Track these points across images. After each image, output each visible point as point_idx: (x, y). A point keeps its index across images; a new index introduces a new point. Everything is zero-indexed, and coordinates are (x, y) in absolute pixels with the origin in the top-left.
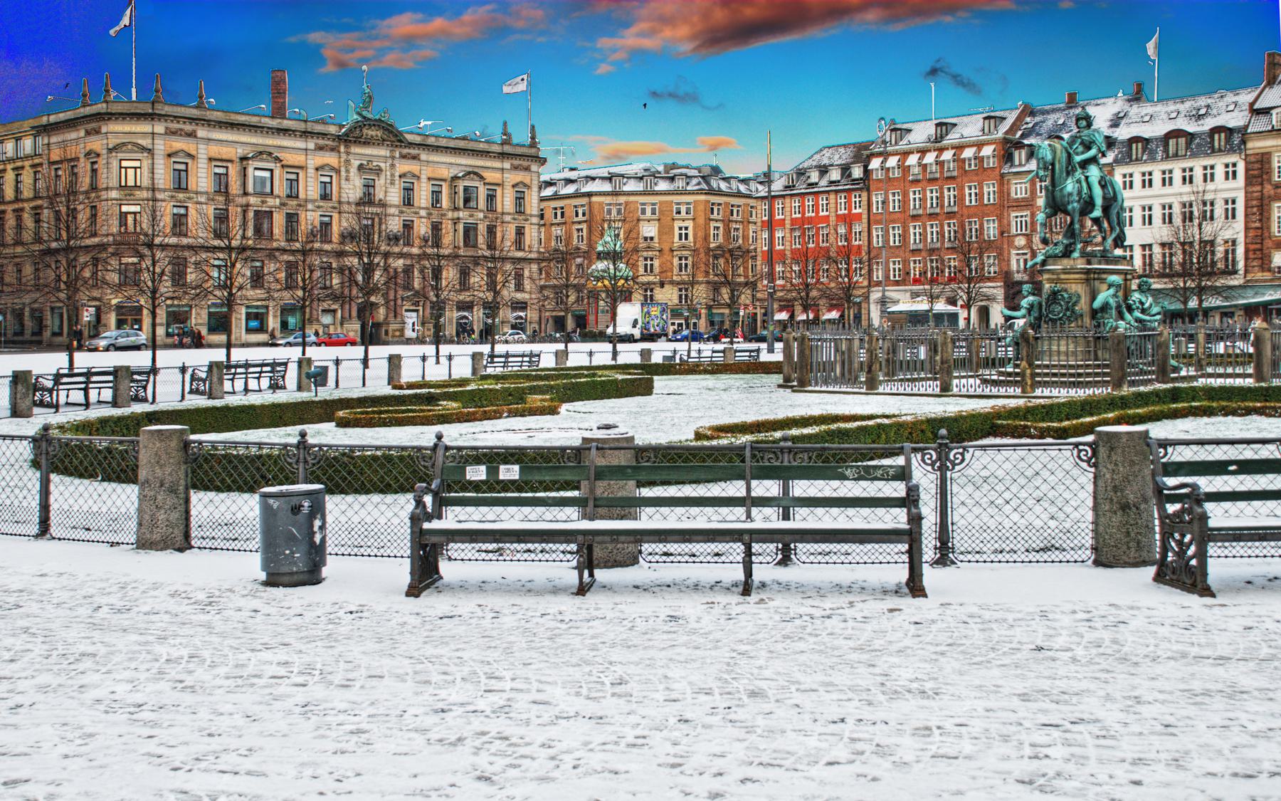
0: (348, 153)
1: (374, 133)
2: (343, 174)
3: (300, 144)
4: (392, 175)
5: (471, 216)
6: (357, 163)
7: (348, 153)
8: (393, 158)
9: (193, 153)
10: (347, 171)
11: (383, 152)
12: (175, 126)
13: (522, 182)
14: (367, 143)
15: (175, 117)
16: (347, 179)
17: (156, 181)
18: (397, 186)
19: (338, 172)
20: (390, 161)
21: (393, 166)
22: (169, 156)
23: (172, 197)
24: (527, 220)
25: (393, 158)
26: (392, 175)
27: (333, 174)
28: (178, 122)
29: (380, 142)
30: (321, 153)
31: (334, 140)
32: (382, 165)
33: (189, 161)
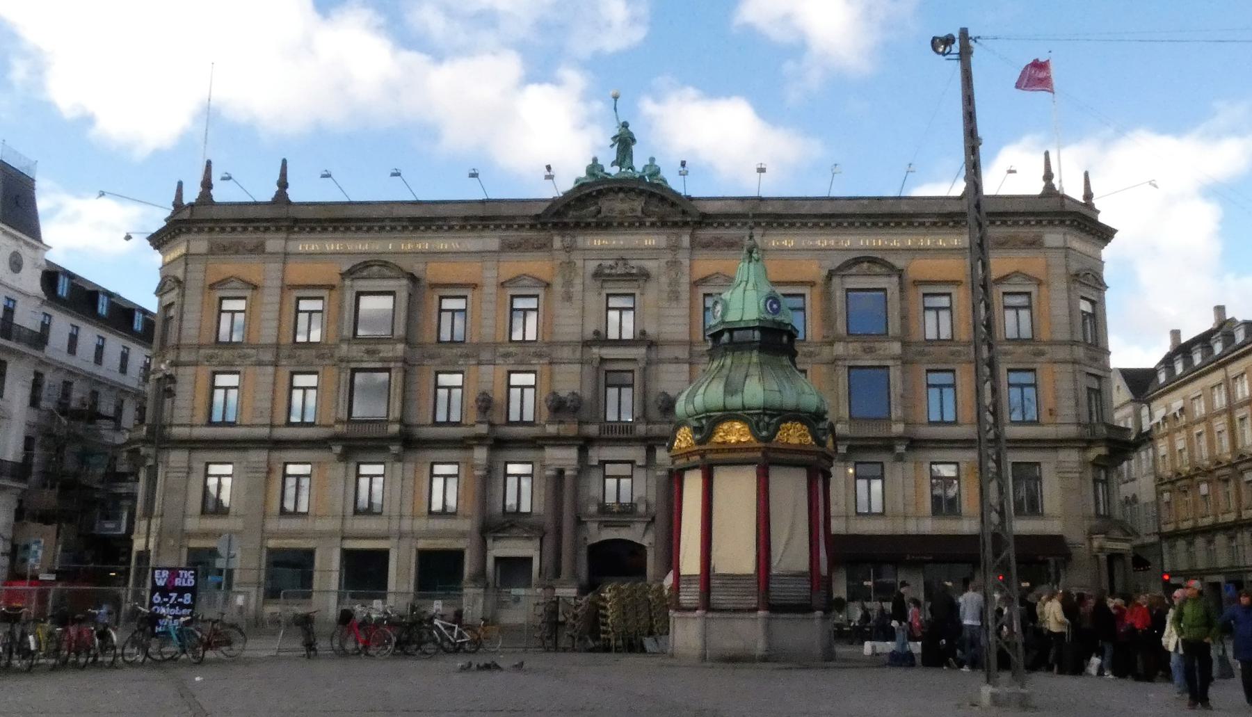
0: (568, 249)
1: (625, 206)
2: (558, 288)
3: (471, 242)
4: (674, 283)
5: (869, 351)
6: (592, 266)
7: (568, 249)
8: (674, 248)
9: (255, 279)
10: (568, 283)
11: (650, 240)
12: (225, 238)
13: (1017, 273)
14: (604, 225)
15: (217, 221)
16: (568, 297)
17: (184, 333)
18: (686, 303)
19: (548, 285)
20: (669, 256)
21: (674, 264)
22: (212, 287)
23: (212, 357)
24: (1041, 353)
25: (674, 248)
26: (674, 283)
27: (540, 292)
28: (223, 230)
29: (635, 224)
30: (513, 255)
31: (532, 227)
32: (650, 265)
33: (248, 293)
